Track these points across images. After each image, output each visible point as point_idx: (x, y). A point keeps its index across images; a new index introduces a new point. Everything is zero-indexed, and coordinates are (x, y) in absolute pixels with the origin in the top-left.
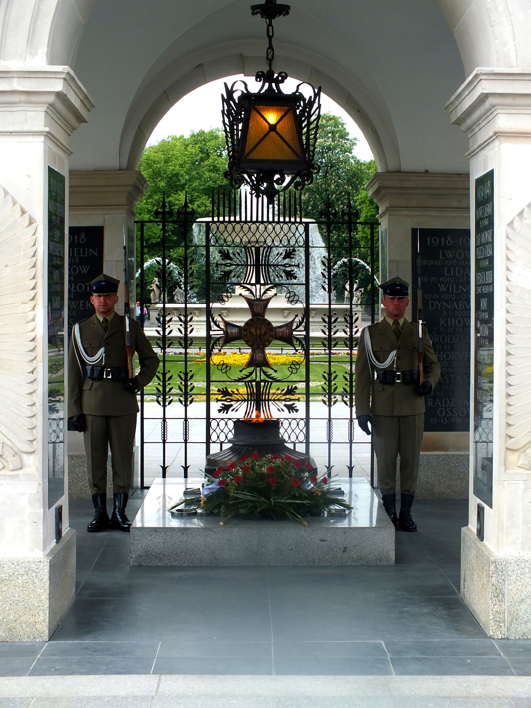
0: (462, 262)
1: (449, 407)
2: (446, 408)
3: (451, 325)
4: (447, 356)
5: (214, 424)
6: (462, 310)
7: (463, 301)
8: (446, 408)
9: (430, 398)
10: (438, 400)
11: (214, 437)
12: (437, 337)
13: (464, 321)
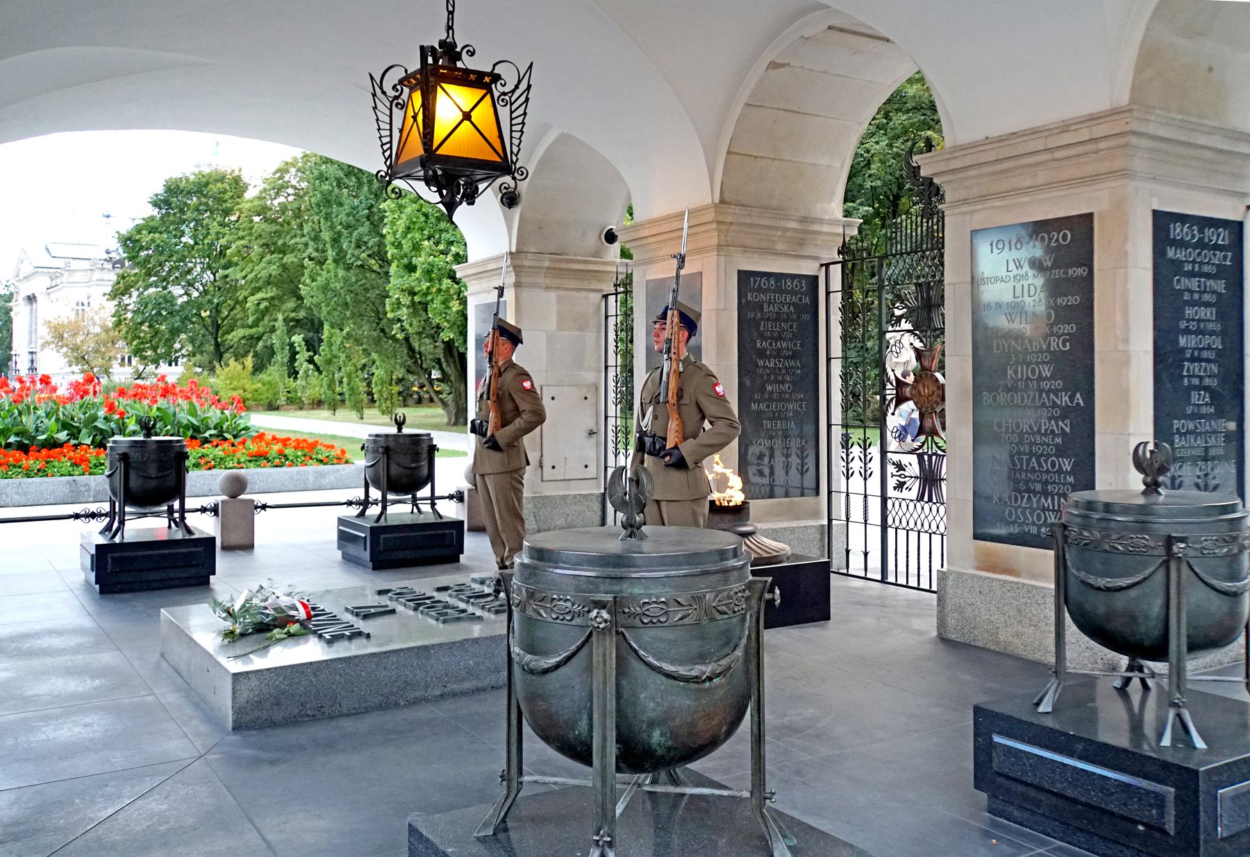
1: (1020, 507)
2: (1016, 509)
5: (890, 503)
8: (1016, 509)
11: (890, 521)
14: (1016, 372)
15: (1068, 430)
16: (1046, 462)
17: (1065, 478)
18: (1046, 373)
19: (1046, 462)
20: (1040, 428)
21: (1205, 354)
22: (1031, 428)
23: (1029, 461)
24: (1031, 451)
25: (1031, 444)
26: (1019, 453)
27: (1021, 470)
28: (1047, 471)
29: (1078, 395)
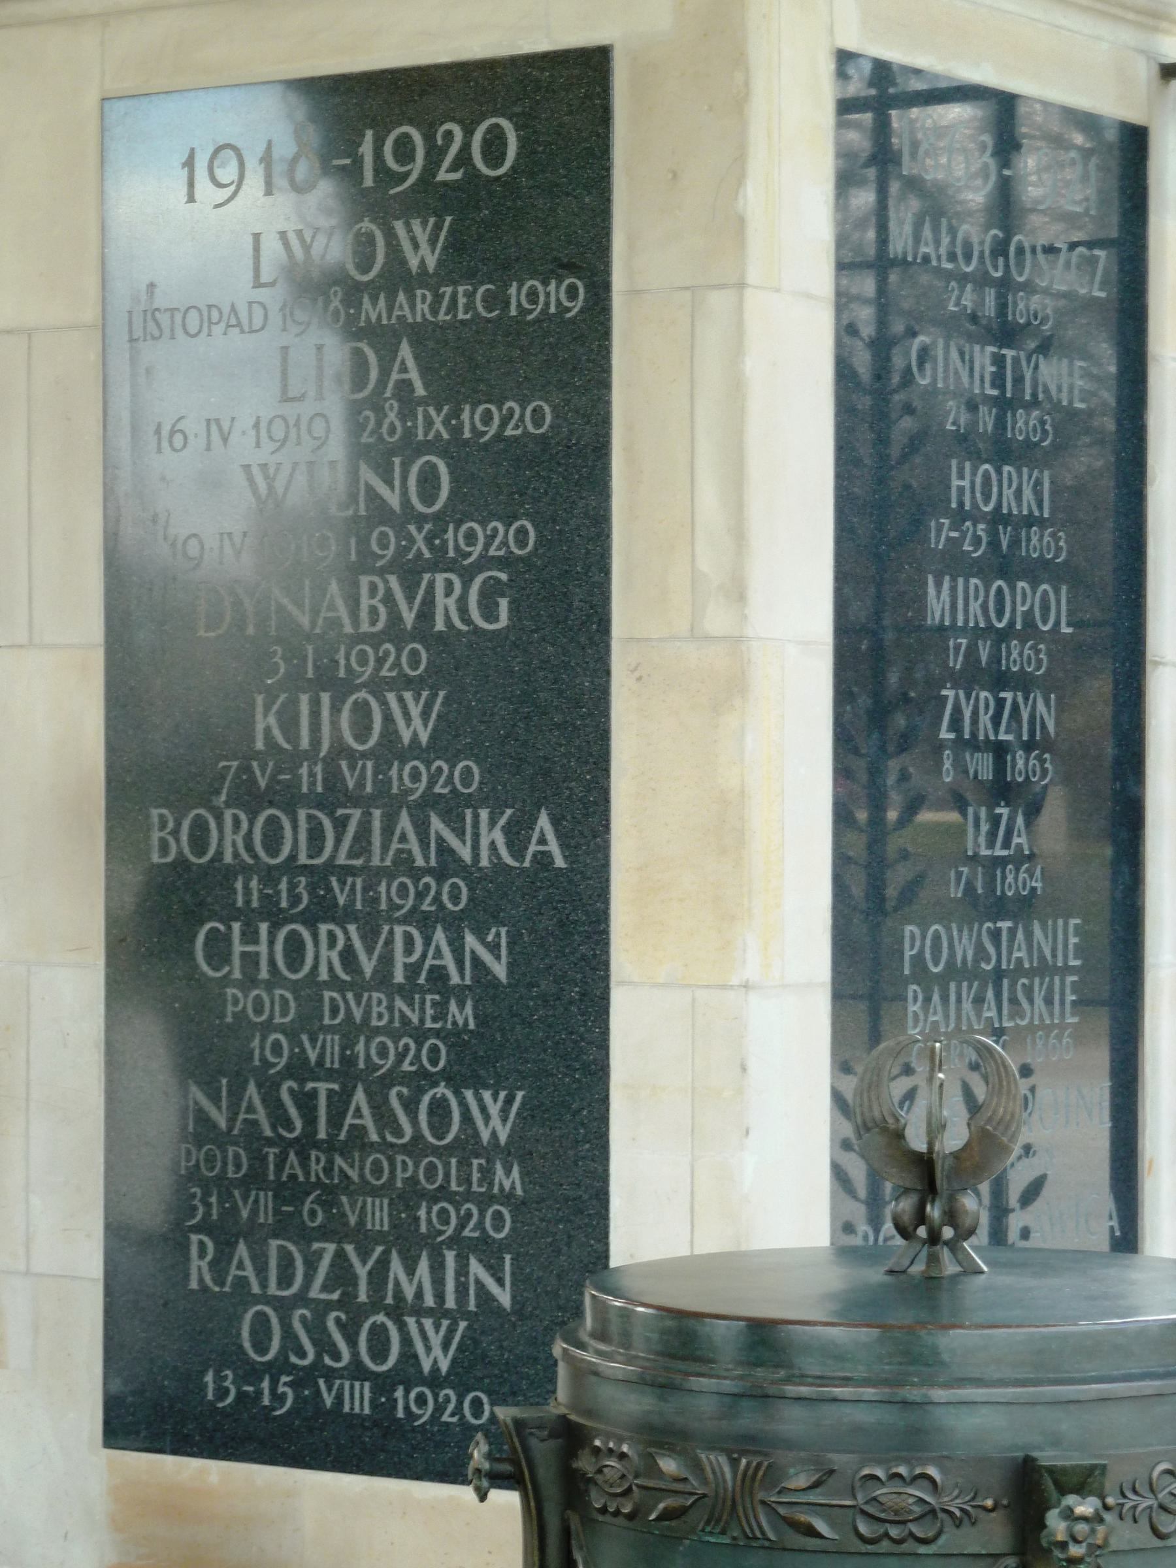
0: (374, 300)
1: (301, 1298)
2: (284, 1307)
3: (316, 742)
4: (295, 947)
6: (375, 640)
7: (382, 572)
9: (197, 1229)
10: (242, 1250)
12: (237, 822)
13: (388, 718)
14: (289, 723)
15: (500, 970)
16: (410, 1106)
17: (487, 1174)
18: (416, 728)
19: (410, 1106)
20: (387, 960)
21: (1017, 656)
22: (348, 957)
23: (340, 1104)
24: (348, 1061)
25: (351, 1031)
26: (299, 1069)
27: (305, 1144)
28: (417, 1147)
29: (544, 822)
